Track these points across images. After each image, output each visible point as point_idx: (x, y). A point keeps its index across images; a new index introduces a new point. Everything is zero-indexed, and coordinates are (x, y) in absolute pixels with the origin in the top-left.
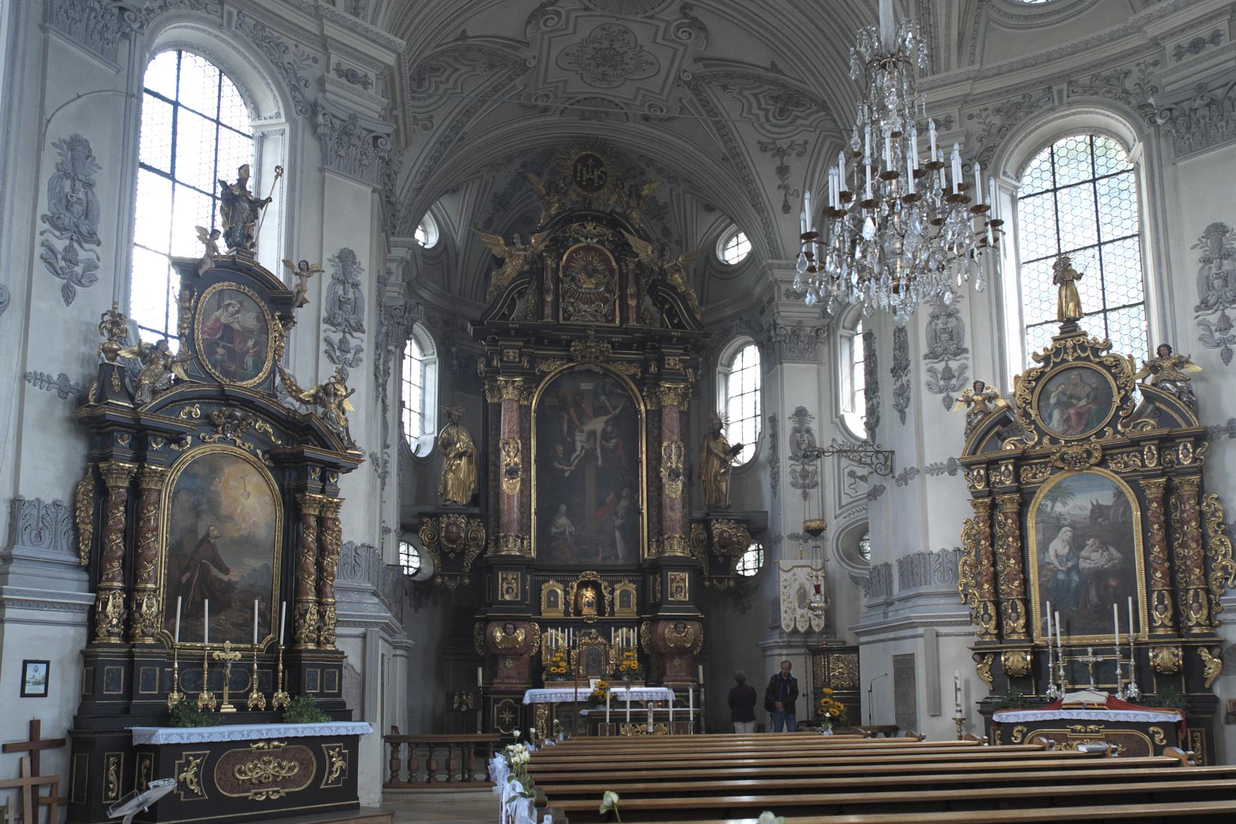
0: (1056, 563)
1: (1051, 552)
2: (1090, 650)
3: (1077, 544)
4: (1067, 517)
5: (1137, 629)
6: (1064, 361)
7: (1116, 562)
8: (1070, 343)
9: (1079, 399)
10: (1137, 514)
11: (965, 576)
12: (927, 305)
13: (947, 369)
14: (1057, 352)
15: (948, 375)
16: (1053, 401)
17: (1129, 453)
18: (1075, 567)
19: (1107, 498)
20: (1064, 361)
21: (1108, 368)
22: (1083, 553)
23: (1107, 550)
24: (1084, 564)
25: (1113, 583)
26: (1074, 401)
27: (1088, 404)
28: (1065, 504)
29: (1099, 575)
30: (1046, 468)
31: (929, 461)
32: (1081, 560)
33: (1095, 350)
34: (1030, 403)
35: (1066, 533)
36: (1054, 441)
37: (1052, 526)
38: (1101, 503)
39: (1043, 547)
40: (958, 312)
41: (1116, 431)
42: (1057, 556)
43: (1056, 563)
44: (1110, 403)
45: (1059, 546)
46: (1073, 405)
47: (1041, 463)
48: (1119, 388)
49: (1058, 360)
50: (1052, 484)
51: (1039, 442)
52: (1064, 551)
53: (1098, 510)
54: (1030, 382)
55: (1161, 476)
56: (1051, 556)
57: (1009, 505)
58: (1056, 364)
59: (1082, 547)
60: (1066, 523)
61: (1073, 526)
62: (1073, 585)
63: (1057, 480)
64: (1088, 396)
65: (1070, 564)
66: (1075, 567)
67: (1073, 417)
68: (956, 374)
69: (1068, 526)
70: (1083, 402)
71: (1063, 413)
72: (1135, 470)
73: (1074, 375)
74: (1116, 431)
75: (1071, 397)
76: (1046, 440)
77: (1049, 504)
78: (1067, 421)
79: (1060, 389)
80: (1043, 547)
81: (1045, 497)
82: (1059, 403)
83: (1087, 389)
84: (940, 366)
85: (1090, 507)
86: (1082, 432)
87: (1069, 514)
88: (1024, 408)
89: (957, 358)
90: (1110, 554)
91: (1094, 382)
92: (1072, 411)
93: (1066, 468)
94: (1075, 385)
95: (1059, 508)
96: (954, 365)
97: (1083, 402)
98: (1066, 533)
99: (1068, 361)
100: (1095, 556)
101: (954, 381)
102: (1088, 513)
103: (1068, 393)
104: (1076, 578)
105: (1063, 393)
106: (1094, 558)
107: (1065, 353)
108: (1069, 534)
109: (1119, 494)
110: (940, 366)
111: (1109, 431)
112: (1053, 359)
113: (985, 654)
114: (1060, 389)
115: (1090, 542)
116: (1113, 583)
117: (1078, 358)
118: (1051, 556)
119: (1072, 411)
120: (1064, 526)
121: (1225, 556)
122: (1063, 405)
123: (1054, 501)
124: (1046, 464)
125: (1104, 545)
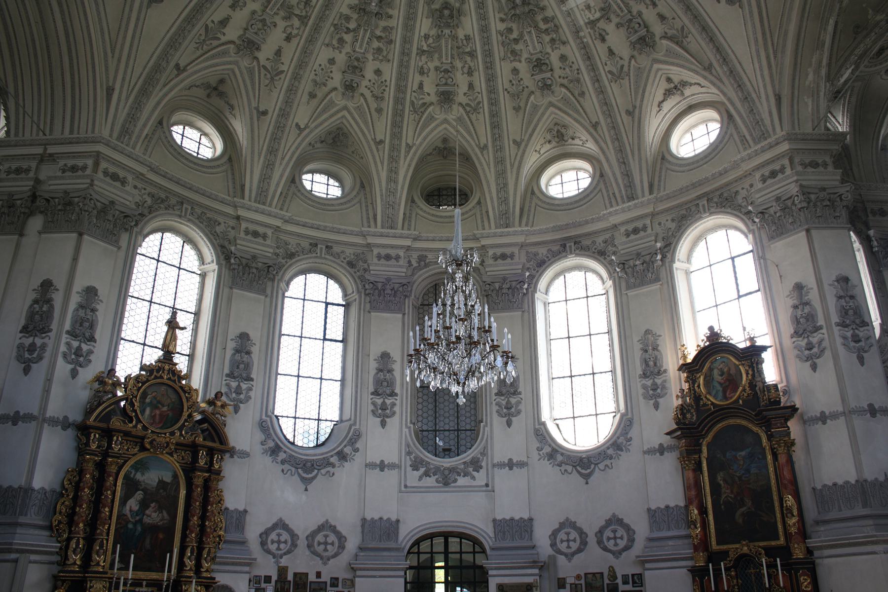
0: (129, 516)
1: (128, 508)
2: (144, 583)
3: (144, 505)
4: (142, 483)
5: (169, 571)
6: (161, 377)
7: (165, 522)
8: (167, 367)
9: (163, 406)
10: (183, 493)
11: (60, 513)
12: (78, 295)
13: (79, 348)
14: (159, 369)
15: (78, 352)
16: (148, 400)
17: (186, 451)
18: (141, 521)
19: (168, 478)
20: (161, 377)
21: (185, 392)
22: (147, 512)
23: (162, 512)
24: (146, 520)
25: (161, 536)
26: (160, 406)
27: (168, 411)
28: (143, 474)
29: (153, 529)
30: (136, 445)
31: (49, 413)
32: (145, 517)
33: (181, 378)
34: (136, 397)
35: (139, 495)
36: (145, 428)
37: (131, 486)
38: (165, 479)
39: (123, 502)
40: (97, 310)
41: (181, 435)
42: (131, 511)
43: (129, 516)
44: (181, 415)
45: (133, 504)
46: (157, 408)
47: (134, 442)
48: (188, 408)
49: (158, 375)
50: (138, 459)
51: (135, 426)
52: (136, 508)
53: (161, 483)
54: (138, 382)
55: (207, 472)
56: (127, 510)
57: (113, 467)
58: (156, 377)
59: (148, 507)
60: (141, 488)
61: (145, 491)
62: (137, 534)
63: (142, 457)
64: (168, 406)
65: (138, 518)
66: (141, 521)
67: (157, 417)
68: (85, 354)
69: (142, 490)
70: (165, 409)
71: (151, 412)
72: (186, 463)
73: (163, 388)
74: (181, 435)
75: (159, 402)
76: (140, 426)
77: (133, 472)
78: (153, 417)
79: (154, 394)
80: (123, 502)
81: (132, 467)
82: (151, 404)
83: (169, 401)
84: (75, 344)
85: (157, 481)
86: (161, 428)
87: (144, 482)
88: (131, 399)
89: (88, 343)
90: (163, 516)
91: (173, 396)
92: (158, 412)
93: (152, 450)
94: (163, 395)
95: (139, 476)
96: (85, 347)
97: (165, 409)
98: (139, 495)
99: (163, 378)
100: (154, 515)
101: (81, 359)
102: (155, 484)
103: (158, 399)
104: (139, 528)
105: (155, 398)
106: (153, 516)
107: (163, 372)
108: (141, 496)
109: (175, 476)
110: (75, 344)
111: (178, 434)
112: (155, 373)
113: (66, 580)
114: (154, 394)
115: (153, 505)
116: (161, 536)
117: (169, 379)
118: (127, 510)
119: (158, 412)
120: (139, 490)
121: (221, 529)
122: (154, 407)
123: (137, 470)
124: (137, 443)
125: (160, 509)
